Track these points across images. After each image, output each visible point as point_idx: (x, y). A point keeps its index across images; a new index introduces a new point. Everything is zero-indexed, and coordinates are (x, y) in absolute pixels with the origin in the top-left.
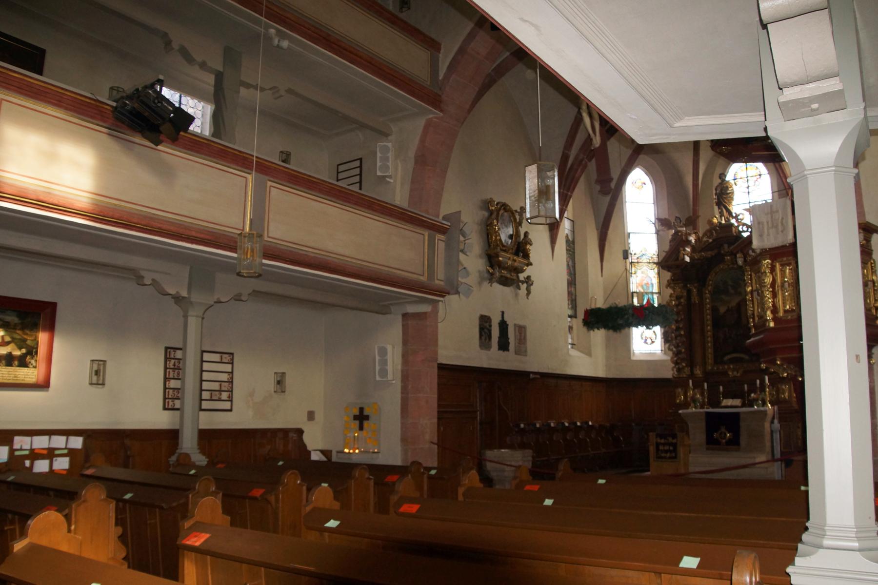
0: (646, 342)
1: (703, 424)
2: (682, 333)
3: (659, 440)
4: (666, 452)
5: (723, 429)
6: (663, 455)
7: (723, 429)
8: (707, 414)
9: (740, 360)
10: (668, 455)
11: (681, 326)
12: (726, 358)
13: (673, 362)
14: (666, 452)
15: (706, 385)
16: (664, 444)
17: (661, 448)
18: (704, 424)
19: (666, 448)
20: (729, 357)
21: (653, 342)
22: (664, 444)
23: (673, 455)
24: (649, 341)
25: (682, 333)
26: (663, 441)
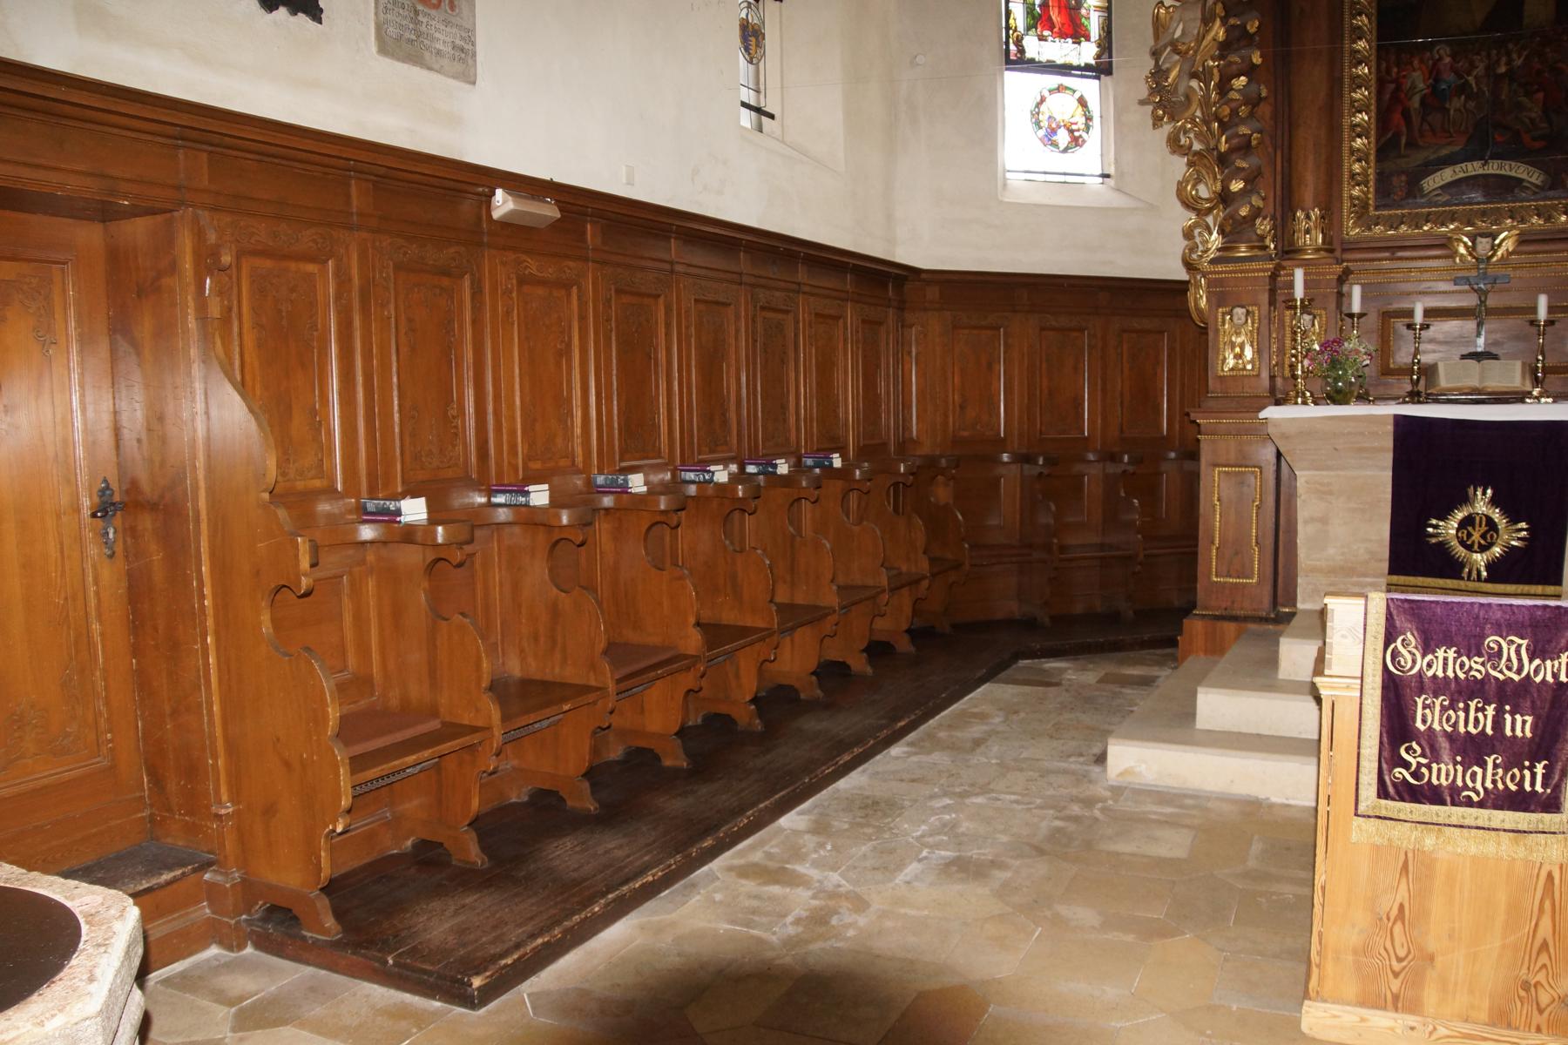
0: (1049, 140)
1: (1380, 476)
2: (1257, 59)
3: (1412, 659)
4: (1472, 749)
5: (1481, 504)
6: (1443, 773)
7: (1481, 504)
8: (1400, 421)
9: (1503, 187)
10: (1488, 775)
11: (1252, 27)
12: (1433, 182)
13: (1189, 203)
14: (1472, 749)
15: (1357, 292)
16: (1462, 691)
17: (1429, 715)
18: (1382, 477)
19: (1479, 719)
20: (1447, 175)
21: (1076, 141)
22: (1462, 691)
23: (1534, 778)
24: (1063, 137)
25: (1257, 59)
26: (1444, 662)
